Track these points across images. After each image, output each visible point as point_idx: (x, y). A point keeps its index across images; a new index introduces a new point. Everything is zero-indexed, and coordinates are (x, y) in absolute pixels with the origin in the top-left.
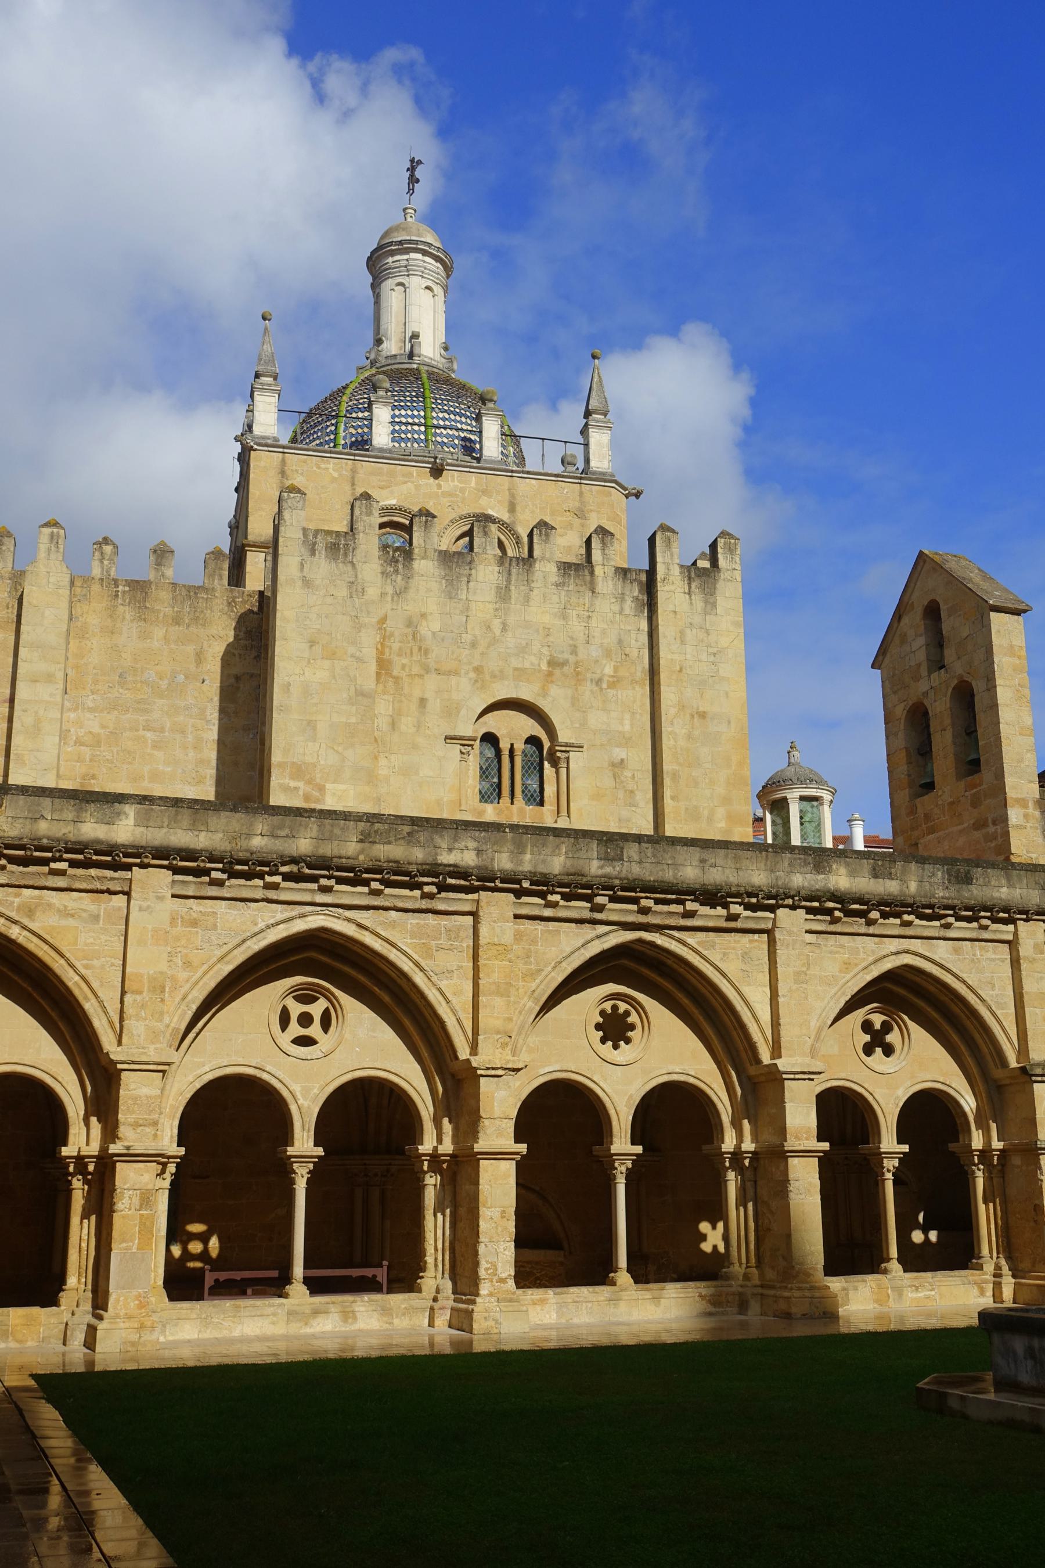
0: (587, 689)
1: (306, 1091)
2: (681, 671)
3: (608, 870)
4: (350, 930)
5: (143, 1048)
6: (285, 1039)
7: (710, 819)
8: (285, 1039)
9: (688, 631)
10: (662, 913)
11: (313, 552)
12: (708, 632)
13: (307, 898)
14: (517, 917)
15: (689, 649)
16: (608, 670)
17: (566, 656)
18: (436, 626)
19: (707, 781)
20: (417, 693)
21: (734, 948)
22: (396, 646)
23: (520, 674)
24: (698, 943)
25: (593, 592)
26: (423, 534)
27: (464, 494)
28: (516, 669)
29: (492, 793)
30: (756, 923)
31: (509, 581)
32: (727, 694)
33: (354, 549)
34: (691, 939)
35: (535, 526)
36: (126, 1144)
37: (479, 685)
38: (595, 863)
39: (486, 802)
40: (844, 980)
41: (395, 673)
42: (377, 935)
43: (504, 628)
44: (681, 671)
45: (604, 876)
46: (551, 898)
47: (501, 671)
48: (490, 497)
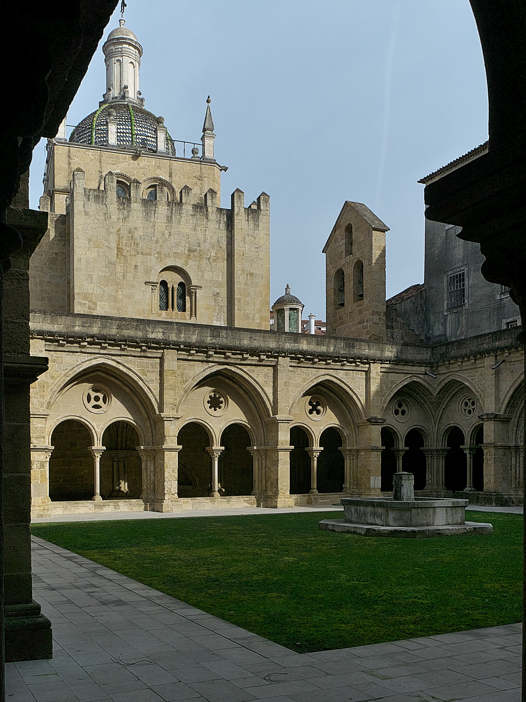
0: (205, 261)
1: (98, 425)
2: (243, 255)
3: (214, 341)
4: (114, 364)
5: (38, 409)
6: (89, 406)
7: (253, 319)
8: (89, 406)
9: (247, 237)
10: (235, 358)
11: (89, 199)
13: (97, 351)
14: (178, 359)
16: (213, 254)
17: (196, 247)
19: (252, 302)
21: (262, 372)
22: (124, 242)
24: (248, 370)
25: (207, 219)
26: (135, 191)
27: (149, 168)
28: (174, 253)
29: (165, 306)
30: (271, 363)
31: (172, 213)
32: (262, 265)
33: (106, 198)
34: (245, 368)
35: (183, 189)
36: (34, 445)
37: (159, 260)
38: (209, 338)
39: (162, 310)
40: (303, 385)
41: (124, 254)
42: (125, 366)
43: (170, 235)
44: (243, 255)
45: (213, 343)
46: (192, 352)
47: (169, 254)
48: (161, 170)
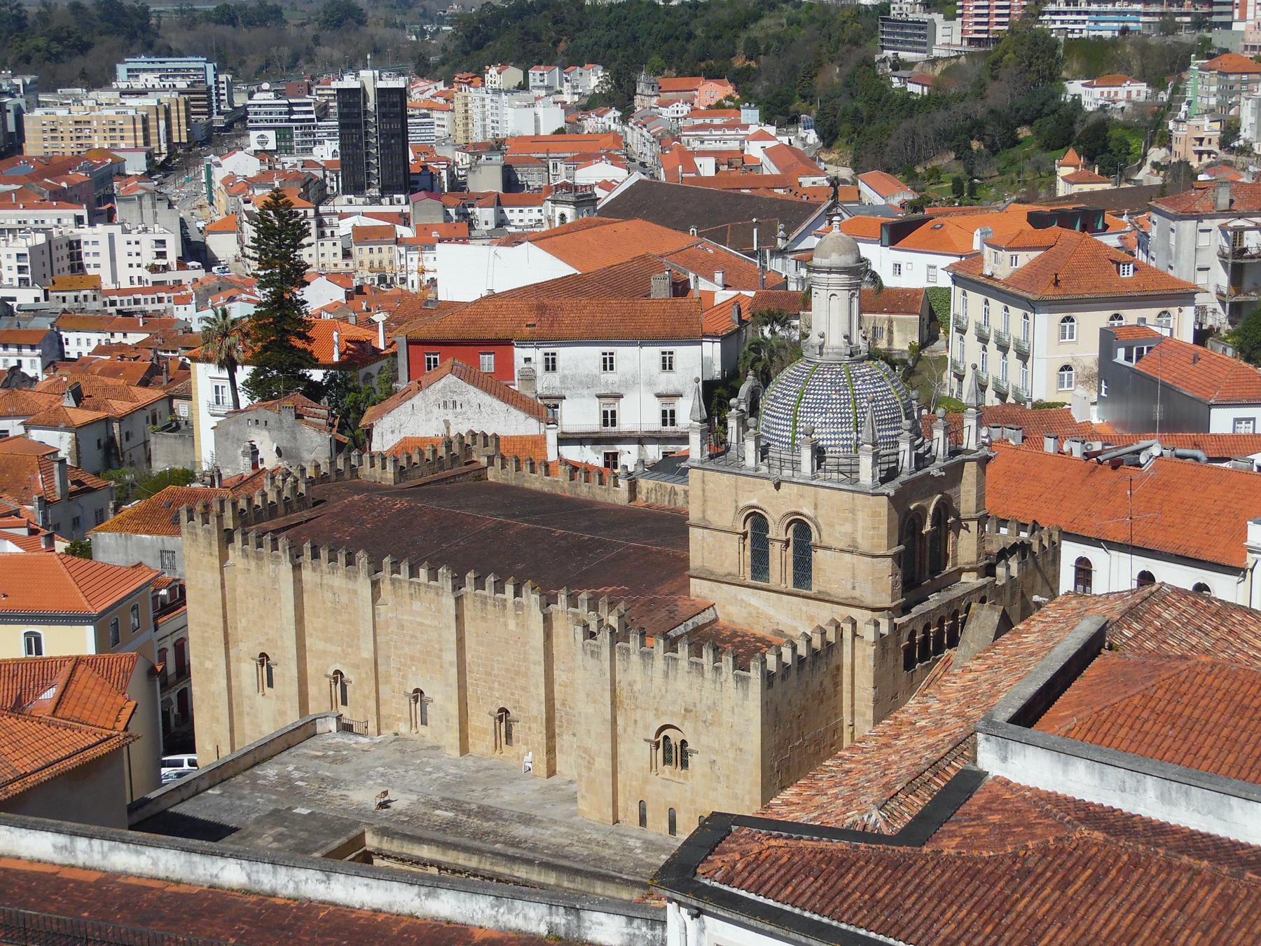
0: (700, 724)
16: (709, 717)
20: (633, 718)
23: (673, 714)
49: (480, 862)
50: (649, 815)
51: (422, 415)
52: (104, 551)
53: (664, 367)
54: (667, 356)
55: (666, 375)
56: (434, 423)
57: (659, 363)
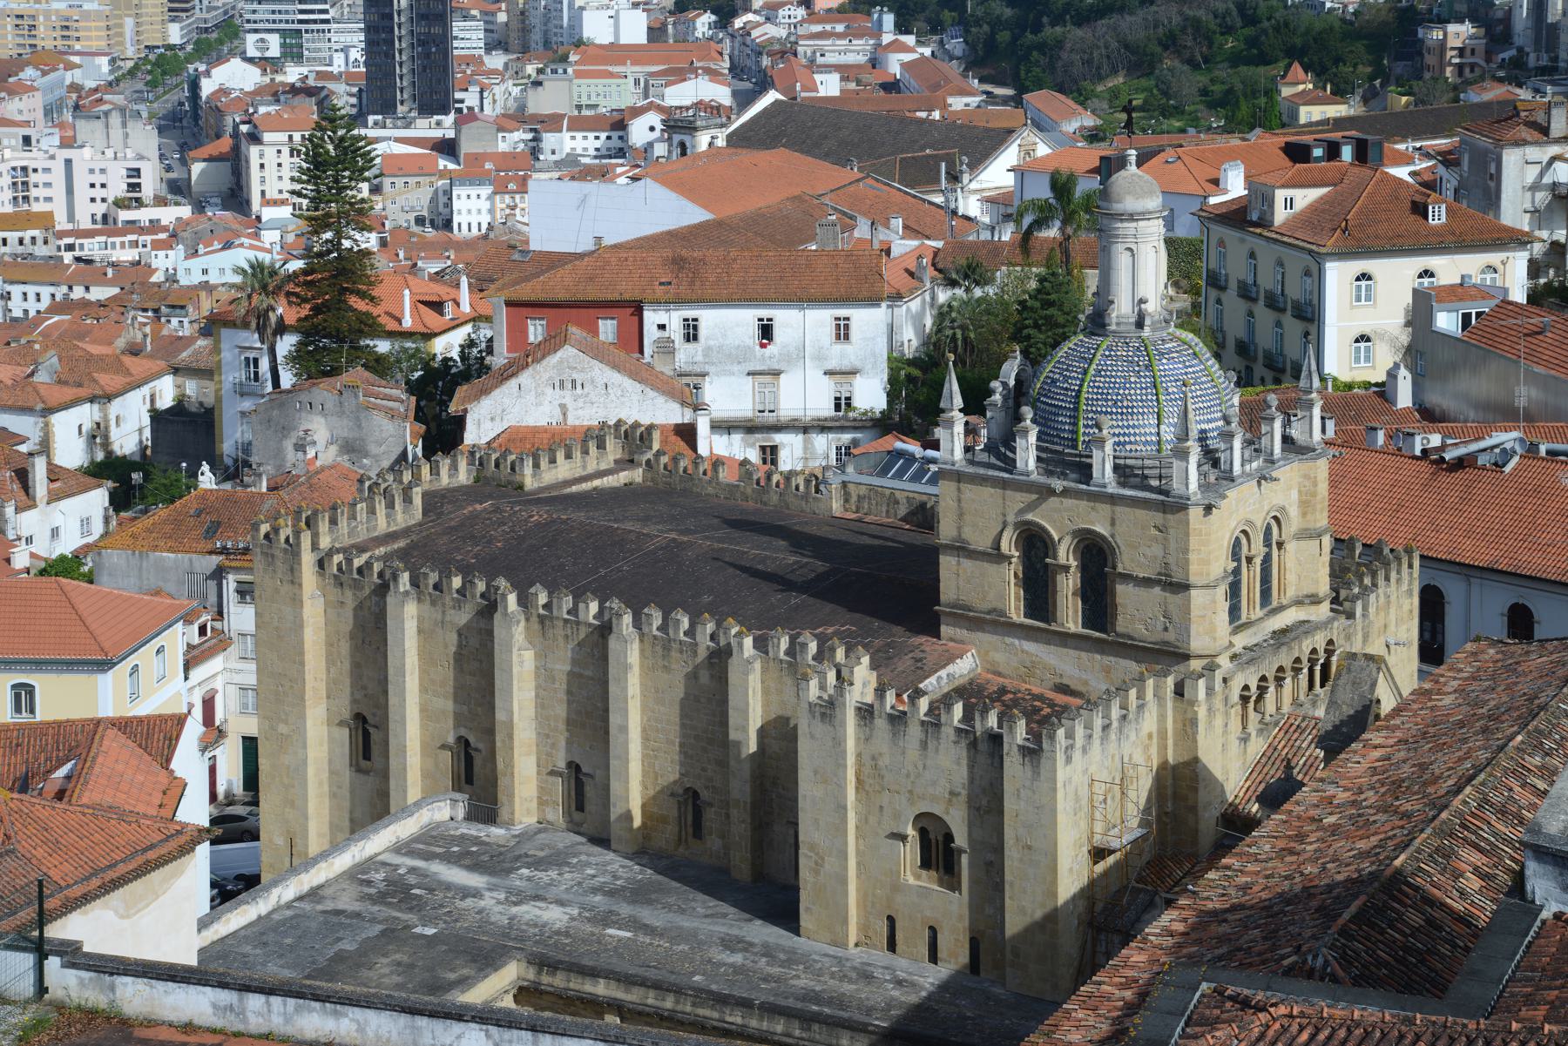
12: (1034, 792)
15: (1022, 803)
18: (887, 761)
49: (677, 1002)
50: (899, 936)
51: (531, 398)
52: (110, 575)
53: (838, 337)
54: (842, 323)
55: (839, 347)
56: (546, 408)
57: (830, 330)
